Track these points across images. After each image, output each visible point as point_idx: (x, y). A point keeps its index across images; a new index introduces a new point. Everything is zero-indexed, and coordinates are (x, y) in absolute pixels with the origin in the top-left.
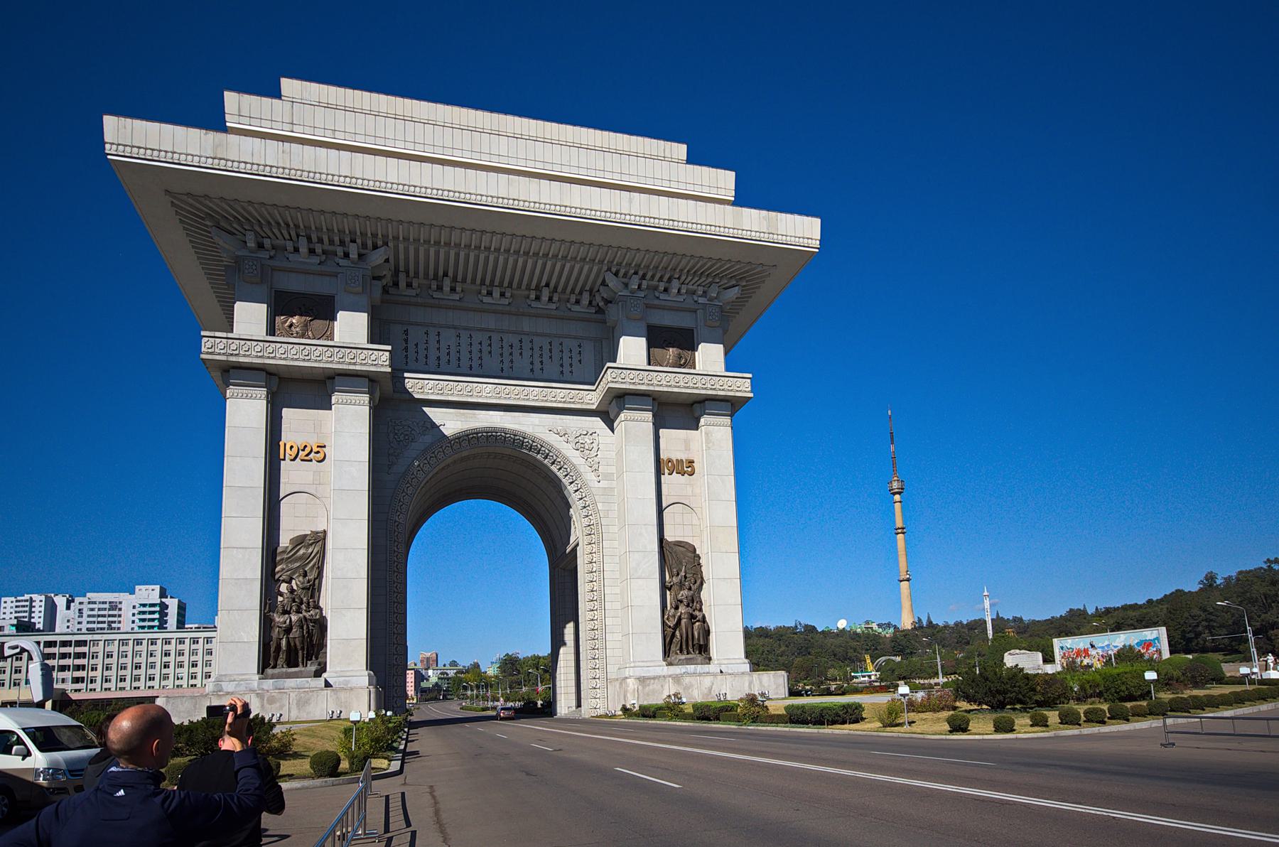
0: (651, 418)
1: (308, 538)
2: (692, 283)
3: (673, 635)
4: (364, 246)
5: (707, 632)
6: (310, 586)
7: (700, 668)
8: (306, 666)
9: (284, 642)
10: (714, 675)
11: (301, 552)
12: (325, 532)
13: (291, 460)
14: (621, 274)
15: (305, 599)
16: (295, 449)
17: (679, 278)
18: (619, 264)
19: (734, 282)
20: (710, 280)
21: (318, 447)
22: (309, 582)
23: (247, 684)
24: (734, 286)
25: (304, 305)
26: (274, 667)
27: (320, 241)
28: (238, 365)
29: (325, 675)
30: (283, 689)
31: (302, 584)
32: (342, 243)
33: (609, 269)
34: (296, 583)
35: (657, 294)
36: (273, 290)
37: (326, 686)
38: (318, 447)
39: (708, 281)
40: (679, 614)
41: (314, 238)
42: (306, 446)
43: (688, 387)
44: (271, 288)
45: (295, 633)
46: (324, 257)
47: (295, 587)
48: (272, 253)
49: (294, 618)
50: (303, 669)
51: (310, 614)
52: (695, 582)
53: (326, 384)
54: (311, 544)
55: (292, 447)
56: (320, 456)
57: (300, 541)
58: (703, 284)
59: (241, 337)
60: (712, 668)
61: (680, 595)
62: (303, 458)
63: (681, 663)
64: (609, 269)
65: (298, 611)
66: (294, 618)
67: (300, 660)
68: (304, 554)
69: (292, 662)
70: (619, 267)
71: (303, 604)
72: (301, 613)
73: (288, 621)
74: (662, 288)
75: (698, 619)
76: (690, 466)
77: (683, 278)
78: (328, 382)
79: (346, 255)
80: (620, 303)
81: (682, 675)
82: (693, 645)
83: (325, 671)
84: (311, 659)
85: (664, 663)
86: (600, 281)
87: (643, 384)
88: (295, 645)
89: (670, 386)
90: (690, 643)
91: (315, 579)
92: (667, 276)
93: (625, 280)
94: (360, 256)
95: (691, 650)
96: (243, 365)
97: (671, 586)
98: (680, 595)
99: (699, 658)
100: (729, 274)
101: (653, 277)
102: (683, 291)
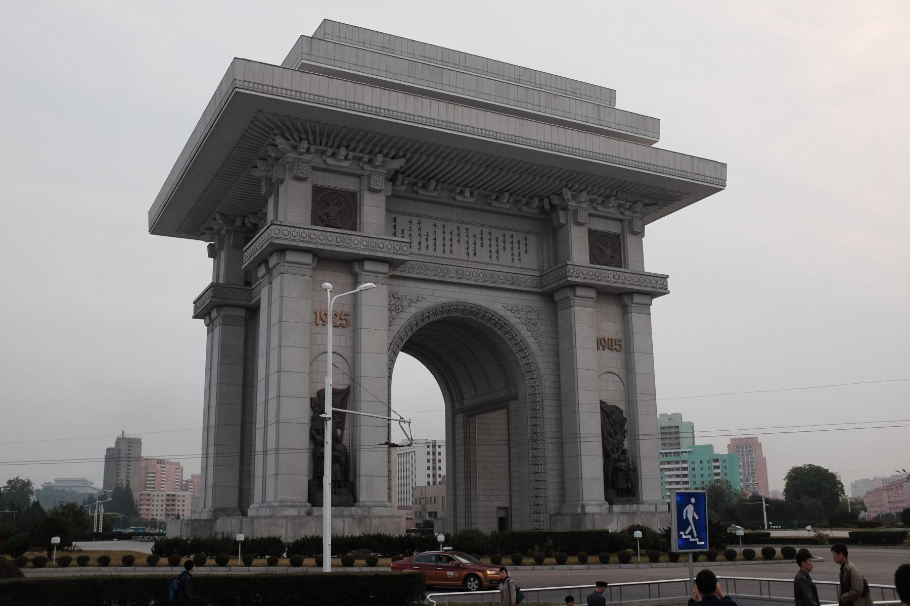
12: (349, 387)
35: (595, 205)
38: (345, 315)
60: (643, 508)
64: (566, 186)
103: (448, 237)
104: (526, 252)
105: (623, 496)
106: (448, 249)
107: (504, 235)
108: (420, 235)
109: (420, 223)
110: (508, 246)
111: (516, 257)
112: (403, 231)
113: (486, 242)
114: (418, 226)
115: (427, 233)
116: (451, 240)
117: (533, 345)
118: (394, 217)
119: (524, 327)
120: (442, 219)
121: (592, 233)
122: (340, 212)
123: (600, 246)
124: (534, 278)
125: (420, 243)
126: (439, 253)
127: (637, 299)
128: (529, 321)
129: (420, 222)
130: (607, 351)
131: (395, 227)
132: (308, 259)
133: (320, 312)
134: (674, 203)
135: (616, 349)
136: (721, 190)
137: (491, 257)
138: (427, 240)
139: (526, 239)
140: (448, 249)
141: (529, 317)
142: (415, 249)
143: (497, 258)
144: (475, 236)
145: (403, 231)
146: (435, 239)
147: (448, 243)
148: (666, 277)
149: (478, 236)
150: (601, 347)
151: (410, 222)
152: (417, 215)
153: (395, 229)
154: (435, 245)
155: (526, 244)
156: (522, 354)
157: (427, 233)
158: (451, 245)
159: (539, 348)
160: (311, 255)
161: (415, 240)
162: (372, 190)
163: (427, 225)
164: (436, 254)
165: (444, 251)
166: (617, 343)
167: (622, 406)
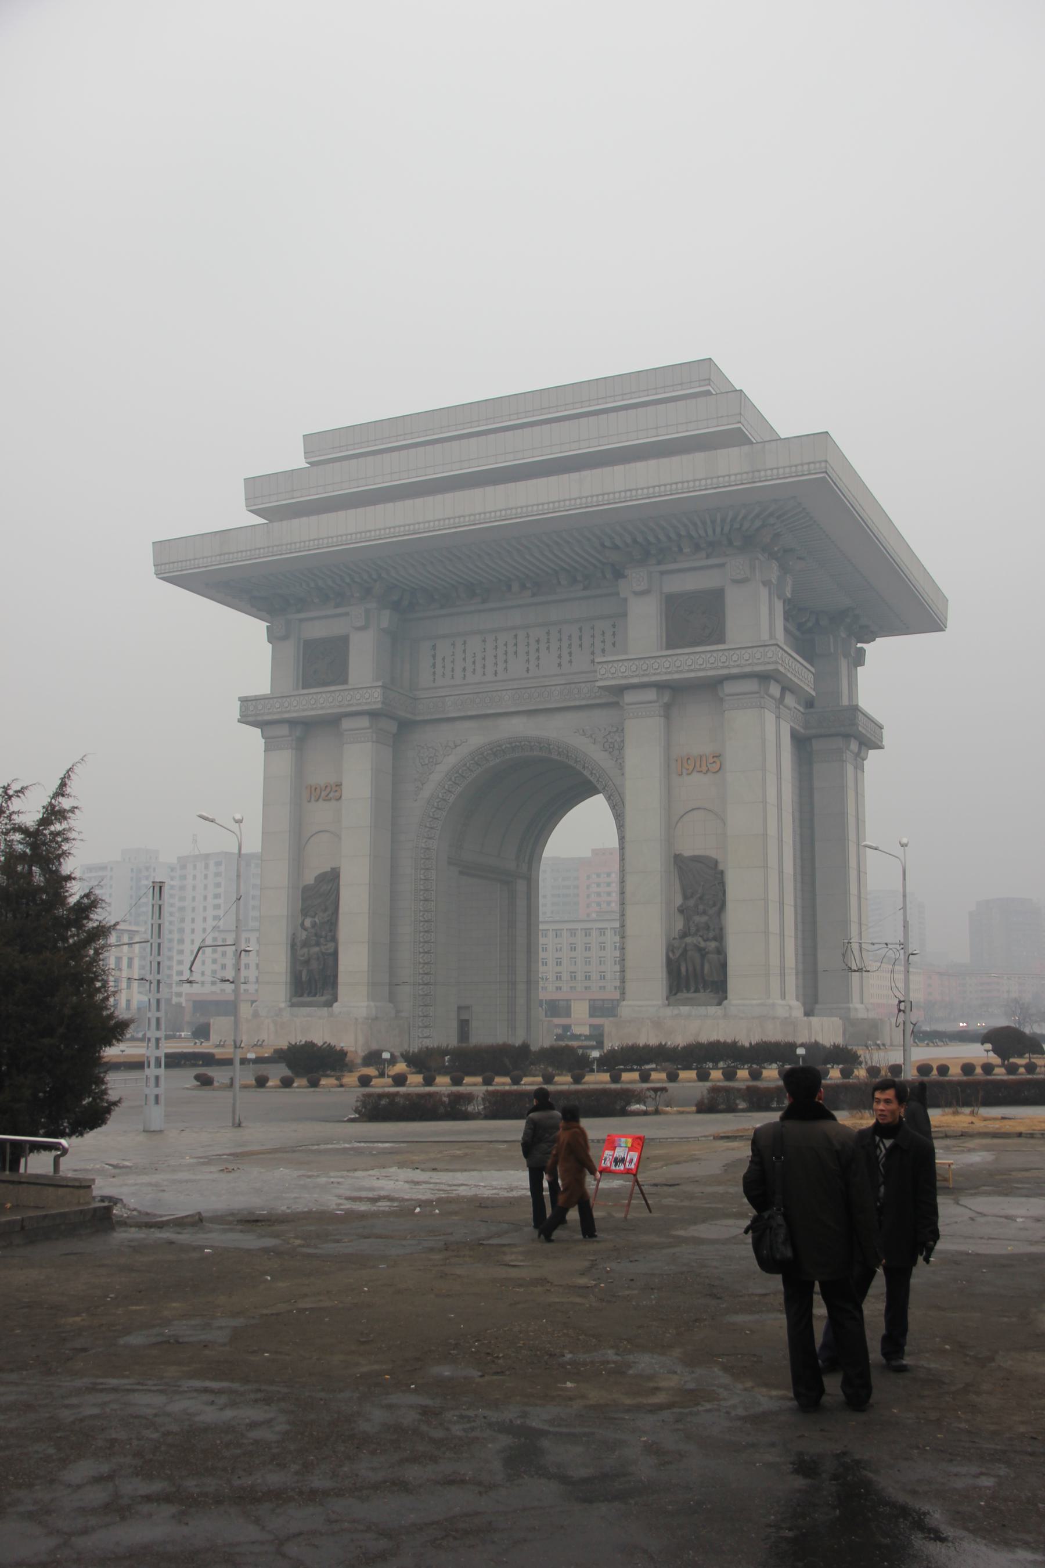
16: (318, 791)
19: (758, 523)
36: (302, 641)
40: (683, 945)
42: (326, 787)
55: (316, 788)
56: (337, 794)
57: (322, 878)
65: (318, 944)
66: (316, 949)
76: (714, 762)
83: (336, 1000)
89: (670, 673)
104: (614, 644)
105: (697, 991)
107: (581, 629)
108: (464, 659)
109: (465, 643)
112: (444, 659)
116: (506, 653)
118: (434, 644)
125: (464, 669)
128: (612, 746)
131: (434, 656)
132: (284, 730)
137: (560, 665)
138: (474, 663)
139: (614, 626)
141: (610, 740)
143: (570, 662)
144: (538, 641)
145: (444, 659)
146: (484, 659)
154: (484, 667)
155: (614, 634)
157: (474, 654)
165: (496, 674)
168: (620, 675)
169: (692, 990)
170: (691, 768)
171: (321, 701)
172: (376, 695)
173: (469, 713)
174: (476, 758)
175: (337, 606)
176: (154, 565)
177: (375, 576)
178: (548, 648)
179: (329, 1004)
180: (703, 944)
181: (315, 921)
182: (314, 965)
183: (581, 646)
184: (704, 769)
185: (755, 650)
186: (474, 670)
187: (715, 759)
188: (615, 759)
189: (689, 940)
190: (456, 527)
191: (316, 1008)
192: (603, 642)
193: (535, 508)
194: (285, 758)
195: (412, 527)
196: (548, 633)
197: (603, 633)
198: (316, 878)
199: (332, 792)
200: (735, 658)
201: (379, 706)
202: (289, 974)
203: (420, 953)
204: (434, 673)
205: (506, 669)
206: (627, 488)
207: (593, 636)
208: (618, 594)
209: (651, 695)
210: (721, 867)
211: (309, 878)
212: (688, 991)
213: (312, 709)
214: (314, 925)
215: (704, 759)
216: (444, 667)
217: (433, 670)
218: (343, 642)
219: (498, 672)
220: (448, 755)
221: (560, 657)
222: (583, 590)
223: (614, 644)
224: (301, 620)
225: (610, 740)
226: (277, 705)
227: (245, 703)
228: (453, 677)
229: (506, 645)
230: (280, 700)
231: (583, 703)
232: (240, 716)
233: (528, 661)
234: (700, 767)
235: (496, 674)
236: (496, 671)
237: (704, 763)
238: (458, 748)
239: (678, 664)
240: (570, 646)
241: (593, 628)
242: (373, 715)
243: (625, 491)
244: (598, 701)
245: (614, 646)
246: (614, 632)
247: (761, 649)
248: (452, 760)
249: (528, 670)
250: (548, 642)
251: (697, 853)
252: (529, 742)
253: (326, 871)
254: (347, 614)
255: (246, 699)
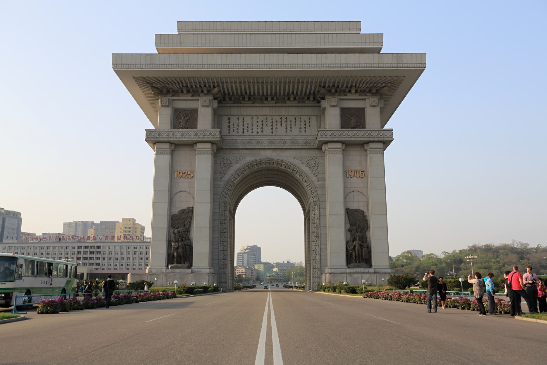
0: (341, 153)
1: (186, 210)
2: (363, 87)
3: (352, 254)
4: (210, 86)
5: (370, 252)
6: (186, 230)
7: (363, 270)
8: (184, 264)
9: (175, 254)
10: (370, 273)
11: (182, 217)
13: (179, 178)
14: (327, 86)
15: (184, 236)
17: (356, 86)
18: (325, 83)
19: (384, 85)
20: (371, 85)
21: (190, 172)
22: (186, 228)
23: (161, 270)
24: (385, 86)
25: (185, 114)
26: (172, 264)
27: (192, 87)
28: (159, 141)
29: (192, 268)
30: (175, 273)
31: (183, 230)
32: (200, 86)
33: (320, 86)
34: (181, 230)
35: (345, 93)
36: (173, 109)
37: (192, 272)
38: (190, 172)
39: (370, 86)
40: (354, 244)
41: (189, 86)
42: (185, 172)
43: (359, 137)
44: (172, 108)
45: (180, 250)
46: (193, 93)
47: (180, 230)
48: (173, 94)
49: (180, 244)
50: (183, 265)
51: (186, 242)
52: (364, 229)
53: (193, 146)
54: (187, 213)
57: (183, 212)
58: (369, 87)
59: (160, 130)
61: (356, 235)
62: (184, 177)
63: (354, 267)
65: (182, 241)
66: (180, 244)
67: (182, 261)
68: (184, 217)
69: (179, 262)
70: (325, 84)
71: (183, 238)
72: (183, 242)
73: (177, 246)
74: (347, 91)
75: (364, 246)
77: (357, 86)
78: (194, 146)
79: (202, 91)
80: (327, 100)
81: (354, 273)
82: (362, 259)
83: (192, 266)
84: (186, 261)
85: (346, 267)
86: (317, 90)
87: (335, 137)
88: (180, 255)
89: (350, 137)
90: (361, 258)
91: (188, 227)
92: (349, 86)
93: (329, 89)
94: (209, 91)
95: (361, 262)
96: (161, 141)
97: (351, 231)
98: (356, 235)
99: (364, 265)
100: (381, 82)
101: (343, 86)
102: (359, 91)
103: (260, 123)
104: (310, 126)
105: (359, 262)
106: (260, 131)
107: (295, 118)
108: (243, 125)
109: (243, 119)
110: (298, 123)
111: (303, 130)
113: (284, 124)
114: (243, 120)
115: (248, 123)
116: (262, 125)
117: (315, 179)
119: (308, 168)
120: (256, 115)
121: (343, 111)
122: (188, 119)
123: (349, 117)
124: (312, 140)
125: (243, 129)
126: (255, 133)
127: (371, 145)
129: (243, 118)
130: (354, 179)
131: (229, 123)
132: (167, 146)
133: (177, 172)
134: (401, 83)
135: (360, 177)
136: (423, 71)
137: (286, 131)
138: (248, 127)
139: (310, 119)
140: (260, 131)
141: (309, 163)
142: (241, 132)
143: (291, 131)
144: (277, 121)
145: (234, 124)
147: (260, 127)
148: (392, 130)
149: (279, 120)
150: (350, 176)
151: (238, 119)
152: (241, 115)
153: (229, 124)
154: (252, 129)
156: (306, 184)
158: (262, 128)
159: (317, 180)
160: (168, 144)
161: (241, 127)
162: (203, 106)
163: (248, 120)
164: (253, 134)
165: (258, 132)
166: (361, 173)
167: (365, 210)
168: (338, 136)
169: (357, 262)
170: (352, 175)
171: (190, 134)
172: (217, 134)
173: (248, 147)
174: (249, 166)
175: (192, 96)
176: (113, 64)
177: (216, 85)
178: (281, 124)
179: (190, 268)
180: (362, 244)
181: (179, 231)
182: (180, 250)
183: (295, 125)
184: (358, 176)
185: (384, 132)
186: (248, 130)
187: (362, 173)
188: (312, 170)
189: (356, 243)
190: (270, 68)
191: (185, 269)
192: (305, 124)
193: (306, 65)
194: (166, 158)
195: (249, 66)
196: (281, 119)
197: (305, 121)
198: (179, 211)
199: (190, 175)
200: (376, 134)
201: (219, 139)
202: (167, 254)
203: (222, 246)
204: (229, 130)
205: (262, 131)
206: (346, 63)
207: (301, 122)
208: (320, 106)
209: (339, 145)
210: (366, 214)
211: (176, 211)
212: (356, 263)
213: (185, 138)
214: (179, 232)
215: (358, 172)
216: (234, 127)
217: (229, 128)
218: (195, 111)
219: (259, 132)
220: (236, 164)
221: (286, 128)
222: (298, 103)
223: (310, 126)
224: (173, 100)
225: (309, 163)
226: (167, 134)
227: (149, 132)
228: (238, 132)
229: (262, 121)
230: (168, 132)
231: (299, 147)
232: (146, 137)
233: (272, 128)
234: (357, 175)
235: (258, 132)
236: (258, 131)
237: (358, 174)
238: (241, 161)
239: (353, 134)
240: (291, 124)
241: (300, 118)
242: (212, 143)
243: (345, 64)
244: (305, 147)
245: (310, 127)
246: (310, 121)
247: (387, 132)
248: (238, 166)
249: (272, 132)
250: (281, 122)
251: (355, 208)
252: (273, 161)
253: (184, 208)
254: (198, 100)
255: (149, 130)
